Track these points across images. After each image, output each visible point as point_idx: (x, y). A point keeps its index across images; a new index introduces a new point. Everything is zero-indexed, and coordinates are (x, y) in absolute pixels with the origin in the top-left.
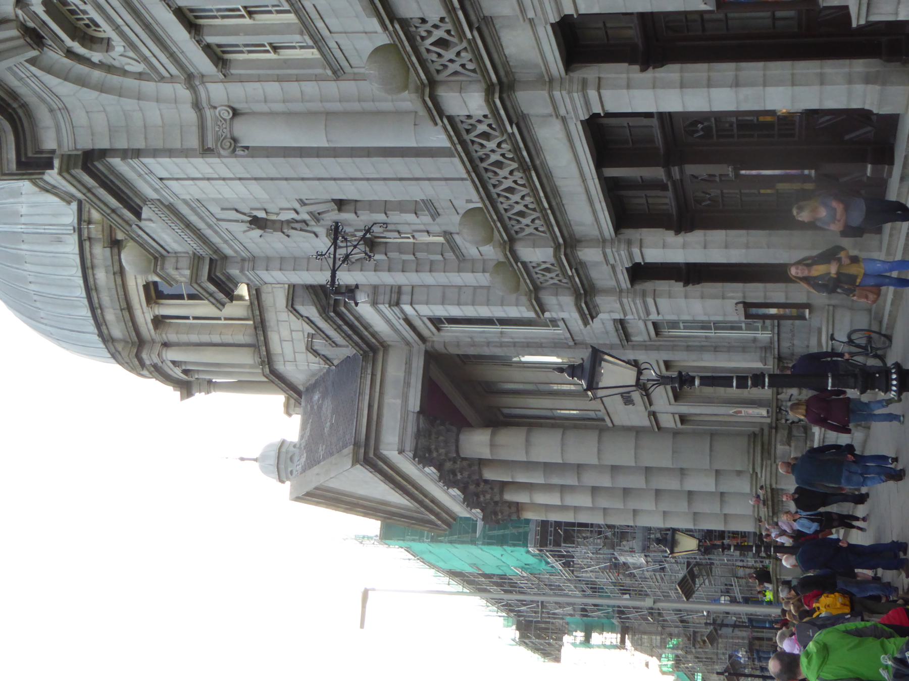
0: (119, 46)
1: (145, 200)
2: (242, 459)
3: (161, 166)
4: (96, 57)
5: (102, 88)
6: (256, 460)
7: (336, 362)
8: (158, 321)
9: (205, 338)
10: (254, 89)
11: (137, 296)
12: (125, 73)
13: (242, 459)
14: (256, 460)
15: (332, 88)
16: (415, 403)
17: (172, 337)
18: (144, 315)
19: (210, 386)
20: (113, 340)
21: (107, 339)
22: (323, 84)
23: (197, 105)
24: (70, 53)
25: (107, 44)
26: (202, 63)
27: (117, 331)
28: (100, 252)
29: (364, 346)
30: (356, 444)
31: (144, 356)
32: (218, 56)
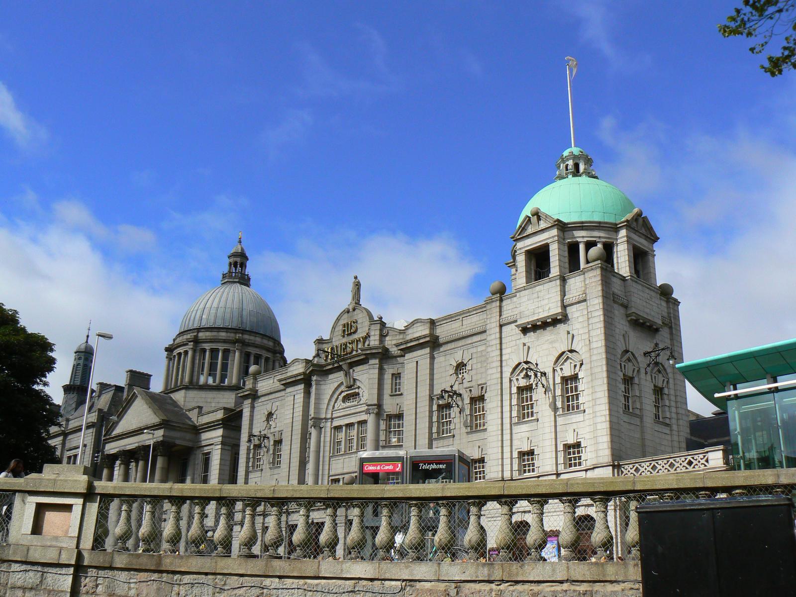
0: (344, 405)
1: (287, 388)
2: (88, 336)
3: (300, 398)
4: (341, 397)
5: (332, 396)
6: (87, 342)
7: (187, 413)
8: (204, 351)
9: (197, 366)
10: (328, 434)
11: (214, 346)
12: (335, 402)
13: (88, 336)
14: (87, 342)
15: (327, 454)
16: (178, 442)
17: (198, 354)
18: (207, 346)
19: (170, 358)
20: (198, 332)
21: (199, 330)
22: (328, 452)
23: (326, 419)
24: (342, 392)
25: (344, 401)
26: (336, 423)
27: (202, 335)
28: (231, 336)
29: (201, 427)
30: (168, 421)
31: (192, 343)
32: (338, 428)
